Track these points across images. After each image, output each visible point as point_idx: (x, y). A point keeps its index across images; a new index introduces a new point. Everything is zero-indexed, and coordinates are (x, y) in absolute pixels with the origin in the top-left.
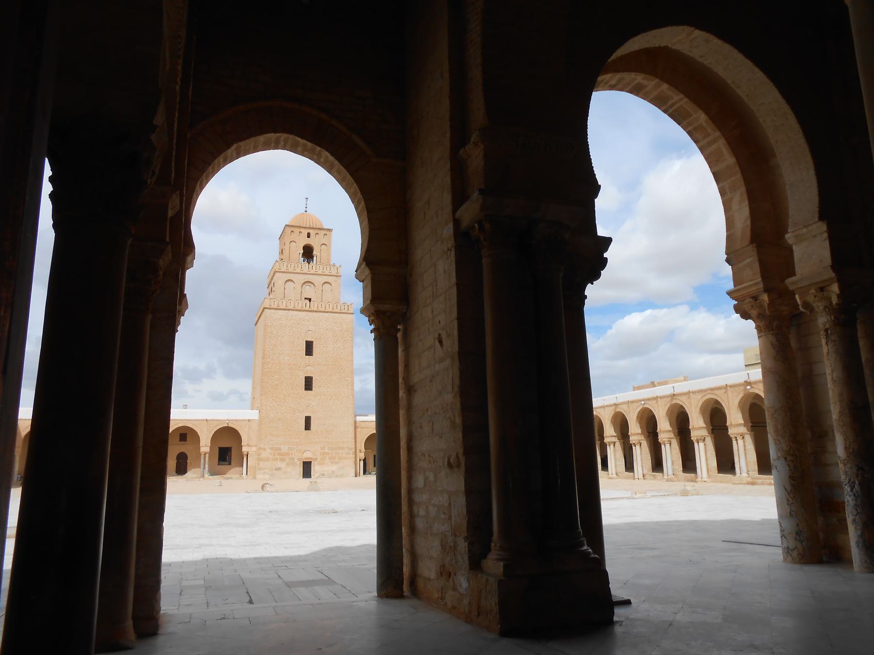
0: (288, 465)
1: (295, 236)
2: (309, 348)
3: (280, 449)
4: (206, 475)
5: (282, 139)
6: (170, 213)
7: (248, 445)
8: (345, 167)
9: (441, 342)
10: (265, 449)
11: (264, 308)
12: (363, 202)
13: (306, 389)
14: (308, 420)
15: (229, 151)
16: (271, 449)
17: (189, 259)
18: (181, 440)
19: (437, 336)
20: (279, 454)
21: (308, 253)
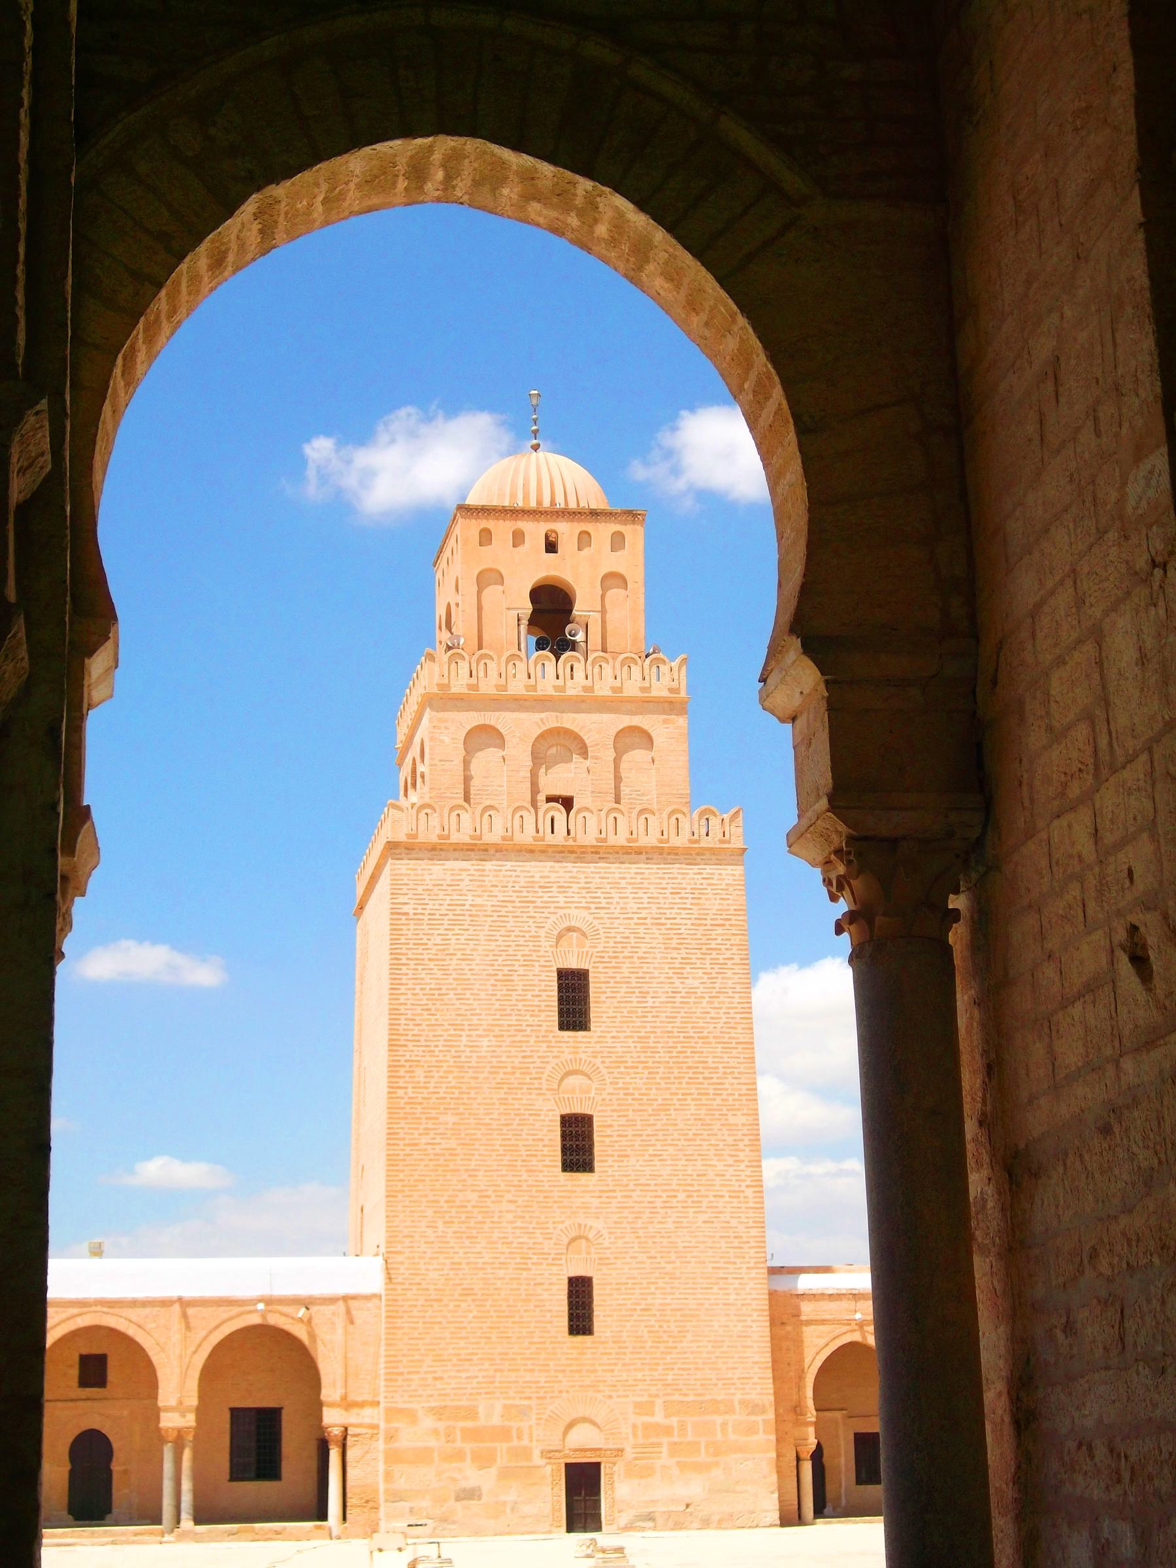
0: (506, 1474)
1: (500, 554)
2: (573, 1000)
3: (472, 1413)
4: (187, 1523)
5: (437, 157)
6: (18, 489)
8: (698, 254)
9: (1140, 961)
10: (412, 1416)
11: (392, 848)
12: (778, 393)
14: (580, 1293)
15: (231, 228)
16: (438, 1412)
17: (97, 665)
18: (84, 1382)
19: (1121, 935)
20: (472, 1435)
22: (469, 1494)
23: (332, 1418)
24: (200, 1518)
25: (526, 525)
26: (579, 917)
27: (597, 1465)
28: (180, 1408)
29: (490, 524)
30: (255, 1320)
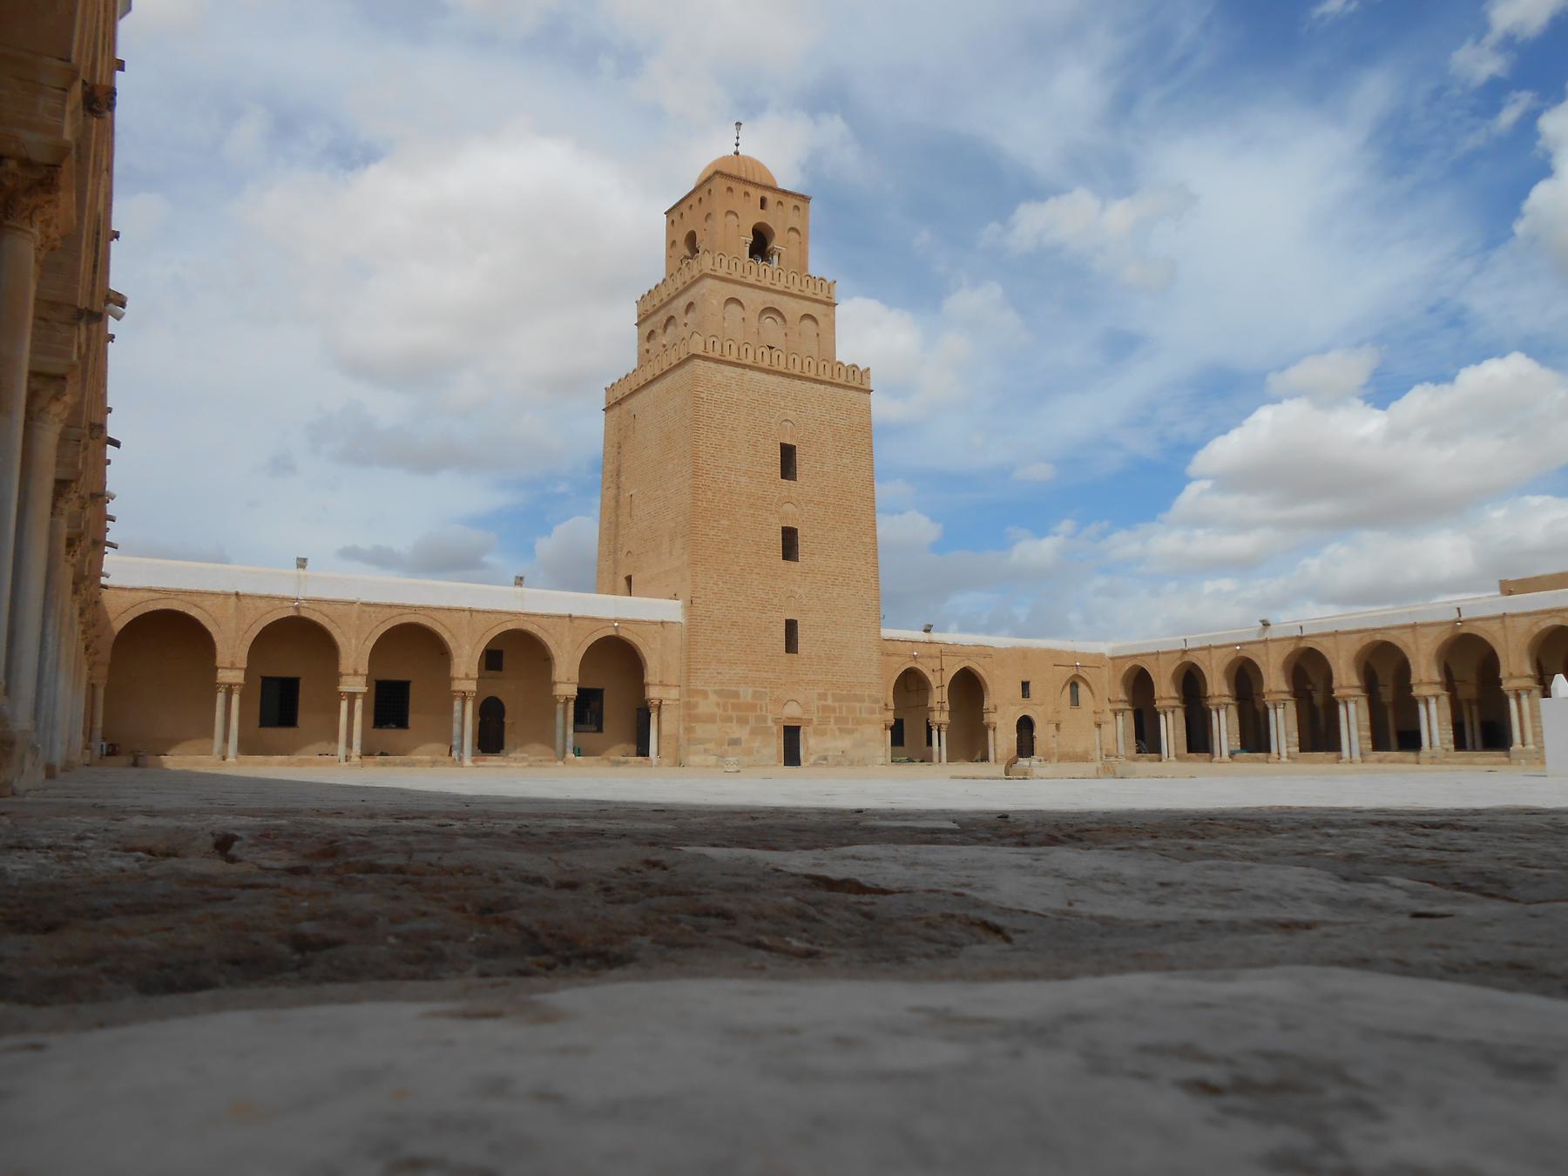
0: (753, 732)
3: (736, 695)
4: (570, 755)
7: (662, 684)
10: (705, 694)
13: (785, 558)
14: (791, 626)
16: (719, 693)
20: (736, 707)
21: (760, 245)
22: (735, 742)
23: (653, 693)
24: (578, 752)
25: (751, 190)
26: (791, 415)
27: (798, 728)
28: (568, 682)
29: (733, 185)
30: (611, 632)
